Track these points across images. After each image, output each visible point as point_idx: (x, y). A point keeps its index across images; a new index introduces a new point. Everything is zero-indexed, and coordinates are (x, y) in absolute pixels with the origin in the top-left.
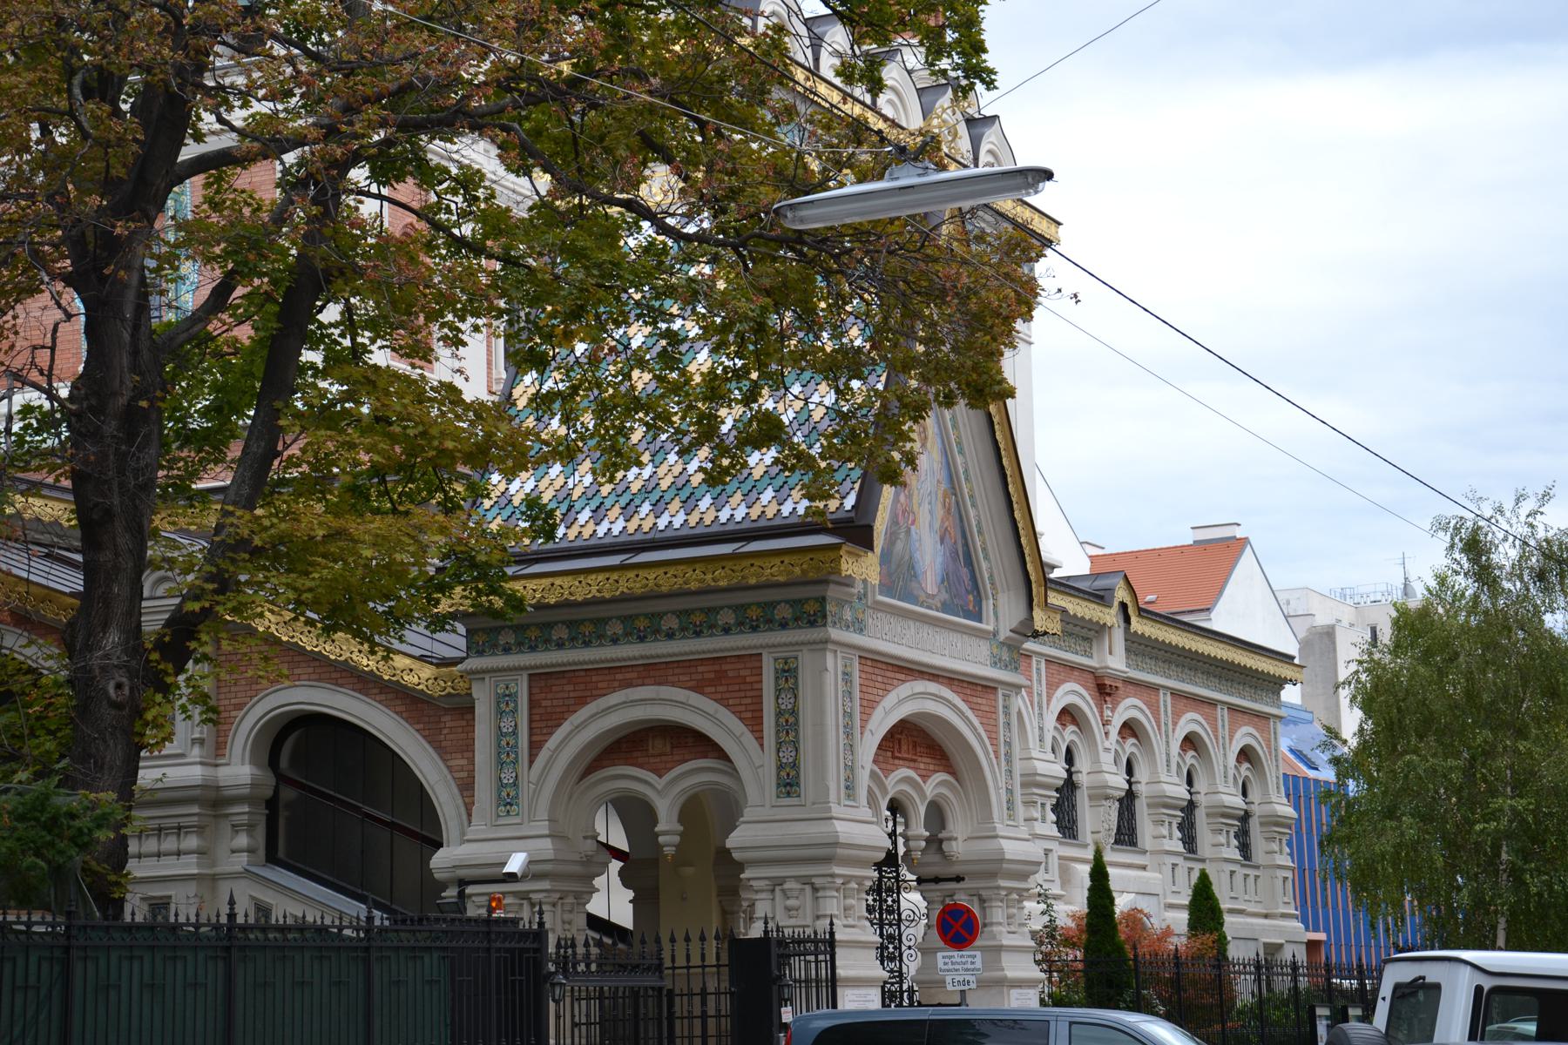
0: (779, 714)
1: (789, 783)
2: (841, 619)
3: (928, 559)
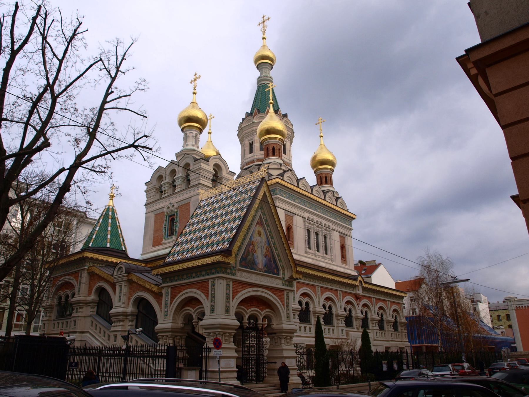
0: (212, 294)
1: (212, 310)
2: (226, 272)
3: (260, 261)
